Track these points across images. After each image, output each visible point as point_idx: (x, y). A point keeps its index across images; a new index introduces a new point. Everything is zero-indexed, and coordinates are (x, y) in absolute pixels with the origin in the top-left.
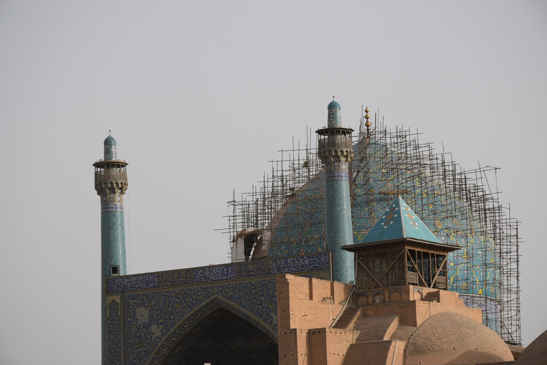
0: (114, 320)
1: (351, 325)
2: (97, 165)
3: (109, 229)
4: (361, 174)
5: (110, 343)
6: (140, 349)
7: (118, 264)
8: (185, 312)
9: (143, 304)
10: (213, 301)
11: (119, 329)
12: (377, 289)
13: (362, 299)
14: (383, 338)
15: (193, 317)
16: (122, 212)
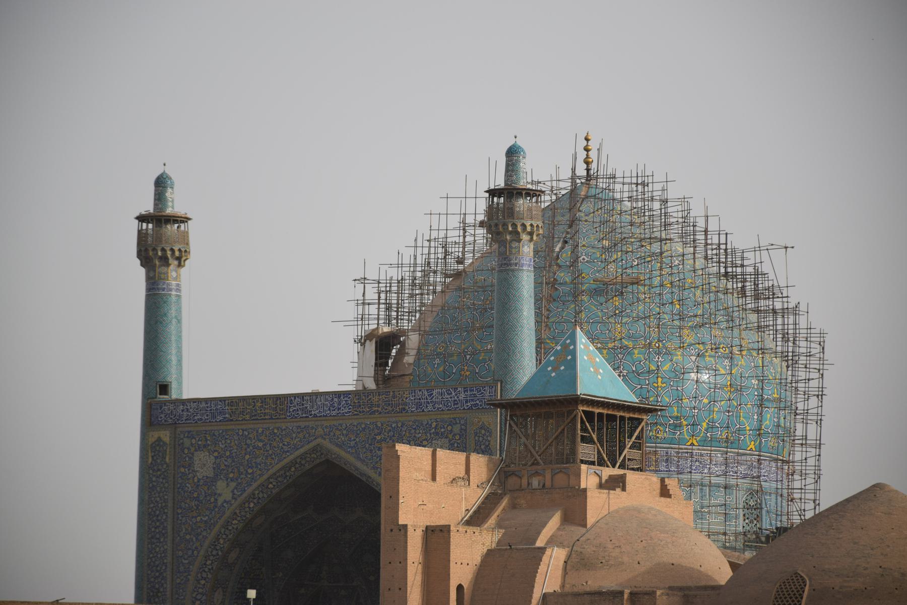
0: (159, 470)
1: (492, 521)
2: (142, 218)
3: (156, 323)
4: (568, 247)
5: (152, 505)
6: (199, 518)
7: (169, 379)
8: (271, 464)
9: (205, 446)
10: (314, 450)
11: (166, 485)
12: (535, 467)
13: (512, 481)
14: (535, 543)
15: (282, 472)
16: (179, 296)
